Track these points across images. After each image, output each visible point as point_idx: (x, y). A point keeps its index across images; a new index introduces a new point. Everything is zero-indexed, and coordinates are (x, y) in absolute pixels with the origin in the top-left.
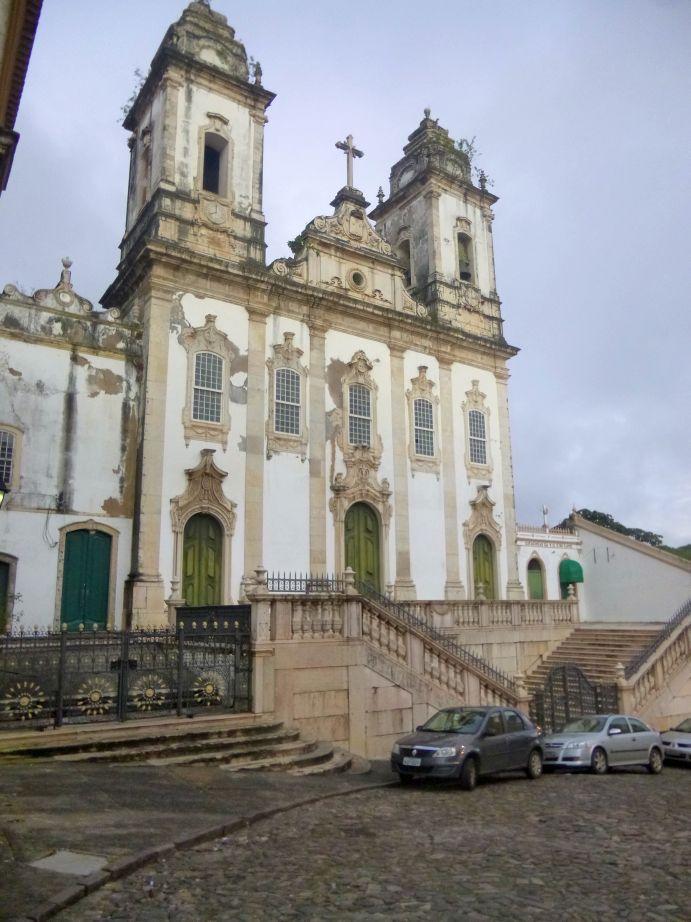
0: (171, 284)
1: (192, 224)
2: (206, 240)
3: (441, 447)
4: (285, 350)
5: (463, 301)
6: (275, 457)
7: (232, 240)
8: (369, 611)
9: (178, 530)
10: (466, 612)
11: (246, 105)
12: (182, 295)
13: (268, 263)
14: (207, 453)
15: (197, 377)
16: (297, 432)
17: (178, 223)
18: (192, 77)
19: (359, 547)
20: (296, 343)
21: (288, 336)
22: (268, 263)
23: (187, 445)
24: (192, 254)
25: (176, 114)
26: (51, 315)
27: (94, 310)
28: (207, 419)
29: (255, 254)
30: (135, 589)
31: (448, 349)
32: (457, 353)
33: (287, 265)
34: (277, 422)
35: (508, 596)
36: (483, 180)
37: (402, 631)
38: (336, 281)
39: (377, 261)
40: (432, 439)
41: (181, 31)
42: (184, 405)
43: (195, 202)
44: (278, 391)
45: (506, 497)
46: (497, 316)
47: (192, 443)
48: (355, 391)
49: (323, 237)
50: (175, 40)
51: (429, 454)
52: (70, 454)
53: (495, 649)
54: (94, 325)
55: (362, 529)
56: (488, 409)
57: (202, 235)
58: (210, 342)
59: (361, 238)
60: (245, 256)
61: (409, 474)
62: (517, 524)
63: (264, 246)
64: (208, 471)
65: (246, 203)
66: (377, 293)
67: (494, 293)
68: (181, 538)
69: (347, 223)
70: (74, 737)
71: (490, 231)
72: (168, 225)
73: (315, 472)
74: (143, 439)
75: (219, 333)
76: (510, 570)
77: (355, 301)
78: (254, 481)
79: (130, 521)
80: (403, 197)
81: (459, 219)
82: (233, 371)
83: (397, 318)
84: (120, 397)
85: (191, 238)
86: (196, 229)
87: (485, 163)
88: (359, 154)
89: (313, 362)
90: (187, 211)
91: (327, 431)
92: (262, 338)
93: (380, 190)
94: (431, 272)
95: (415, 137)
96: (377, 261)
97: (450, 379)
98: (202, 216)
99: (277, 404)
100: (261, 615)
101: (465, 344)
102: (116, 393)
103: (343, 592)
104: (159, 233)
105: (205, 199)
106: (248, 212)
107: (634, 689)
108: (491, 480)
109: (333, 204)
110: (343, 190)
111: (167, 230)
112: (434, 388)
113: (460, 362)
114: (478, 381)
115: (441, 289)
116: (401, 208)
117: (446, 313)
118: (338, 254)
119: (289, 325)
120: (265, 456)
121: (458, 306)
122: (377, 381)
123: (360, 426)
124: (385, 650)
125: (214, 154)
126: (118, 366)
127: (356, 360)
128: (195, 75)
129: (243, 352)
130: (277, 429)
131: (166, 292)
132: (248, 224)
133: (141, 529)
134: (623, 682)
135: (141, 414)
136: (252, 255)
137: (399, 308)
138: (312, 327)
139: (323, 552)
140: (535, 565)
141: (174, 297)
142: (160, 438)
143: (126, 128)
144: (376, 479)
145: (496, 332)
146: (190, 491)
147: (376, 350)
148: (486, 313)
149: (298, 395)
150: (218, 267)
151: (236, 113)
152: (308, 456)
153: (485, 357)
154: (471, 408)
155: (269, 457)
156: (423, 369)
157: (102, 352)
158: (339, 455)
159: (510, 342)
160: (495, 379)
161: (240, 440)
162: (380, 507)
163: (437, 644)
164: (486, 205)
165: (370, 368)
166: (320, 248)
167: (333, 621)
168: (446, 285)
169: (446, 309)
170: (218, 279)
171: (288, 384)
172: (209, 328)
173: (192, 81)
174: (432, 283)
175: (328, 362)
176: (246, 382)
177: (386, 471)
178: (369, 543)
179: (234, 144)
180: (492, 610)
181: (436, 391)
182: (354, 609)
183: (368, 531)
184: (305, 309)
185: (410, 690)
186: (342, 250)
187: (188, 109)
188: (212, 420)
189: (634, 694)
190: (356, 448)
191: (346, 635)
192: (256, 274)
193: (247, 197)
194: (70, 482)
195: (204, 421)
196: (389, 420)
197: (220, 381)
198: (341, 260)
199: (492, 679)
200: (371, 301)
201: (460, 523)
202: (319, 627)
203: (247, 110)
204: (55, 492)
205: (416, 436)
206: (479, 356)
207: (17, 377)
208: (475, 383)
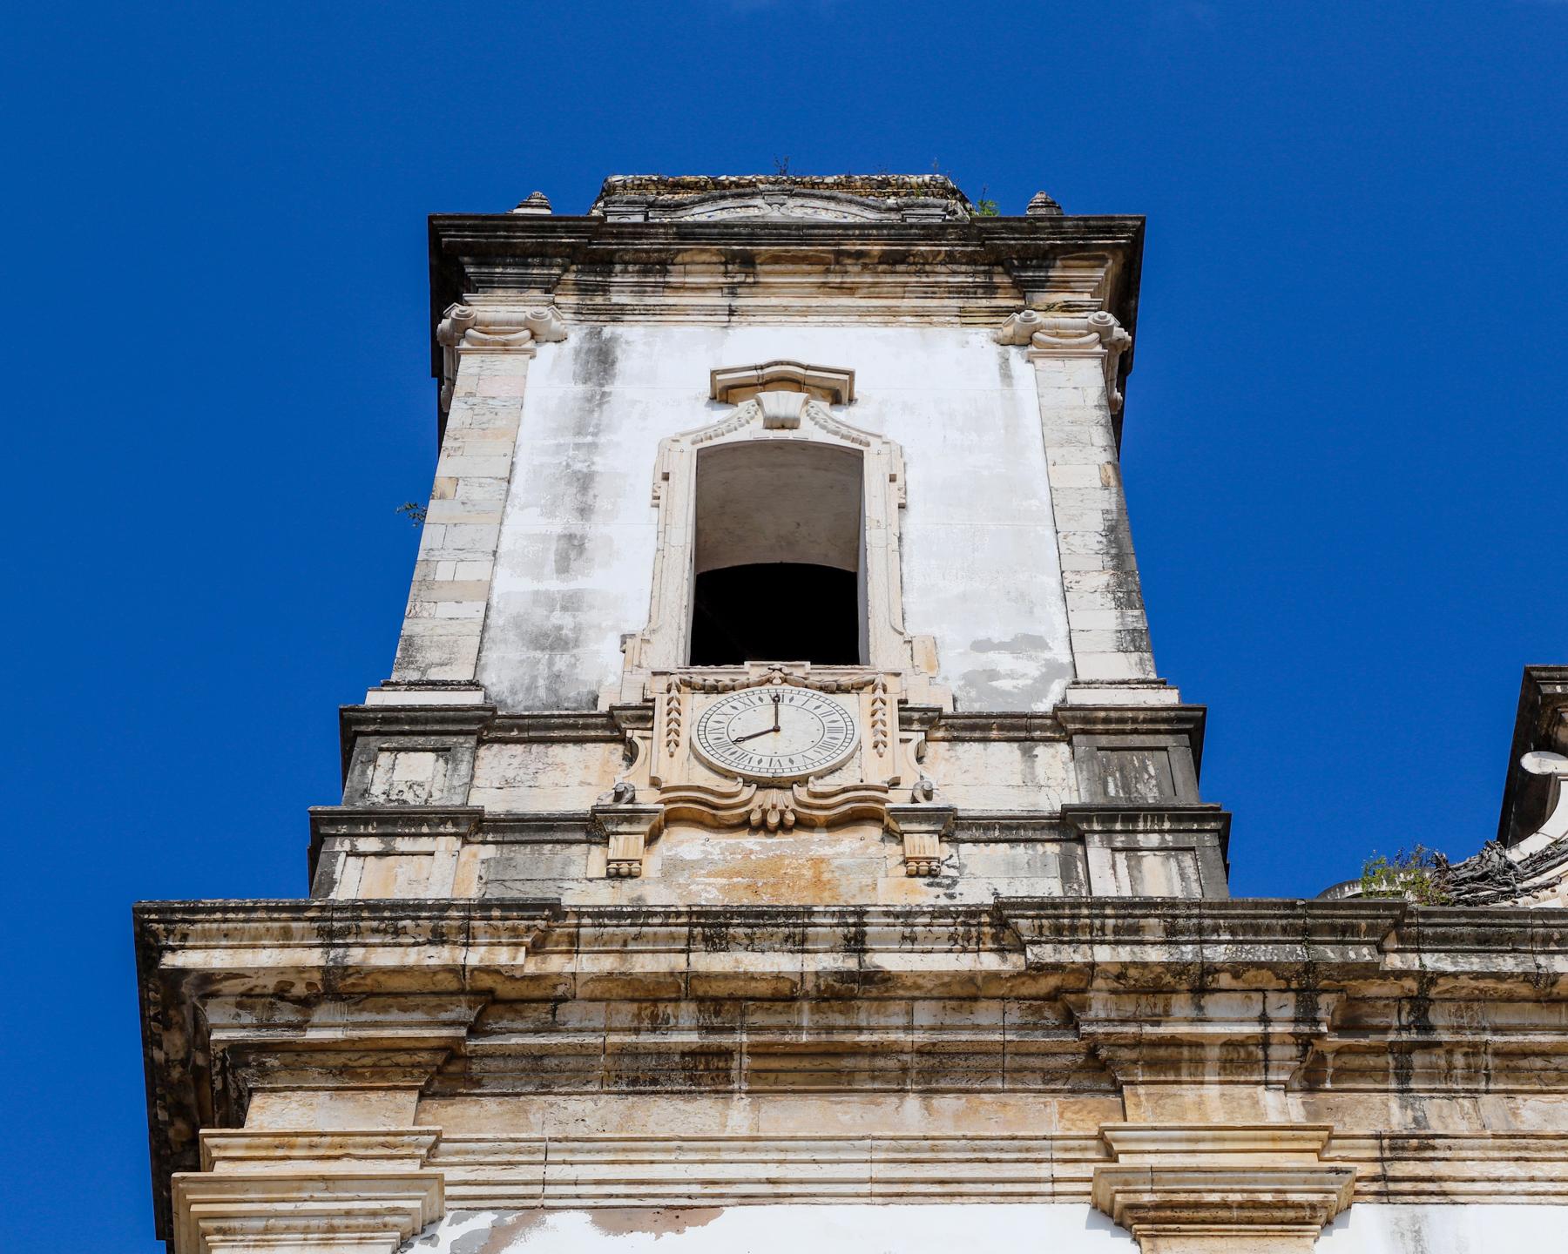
7: (924, 843)
170: (831, 1070)
173: (617, 314)
193: (1030, 643)
203: (981, 339)
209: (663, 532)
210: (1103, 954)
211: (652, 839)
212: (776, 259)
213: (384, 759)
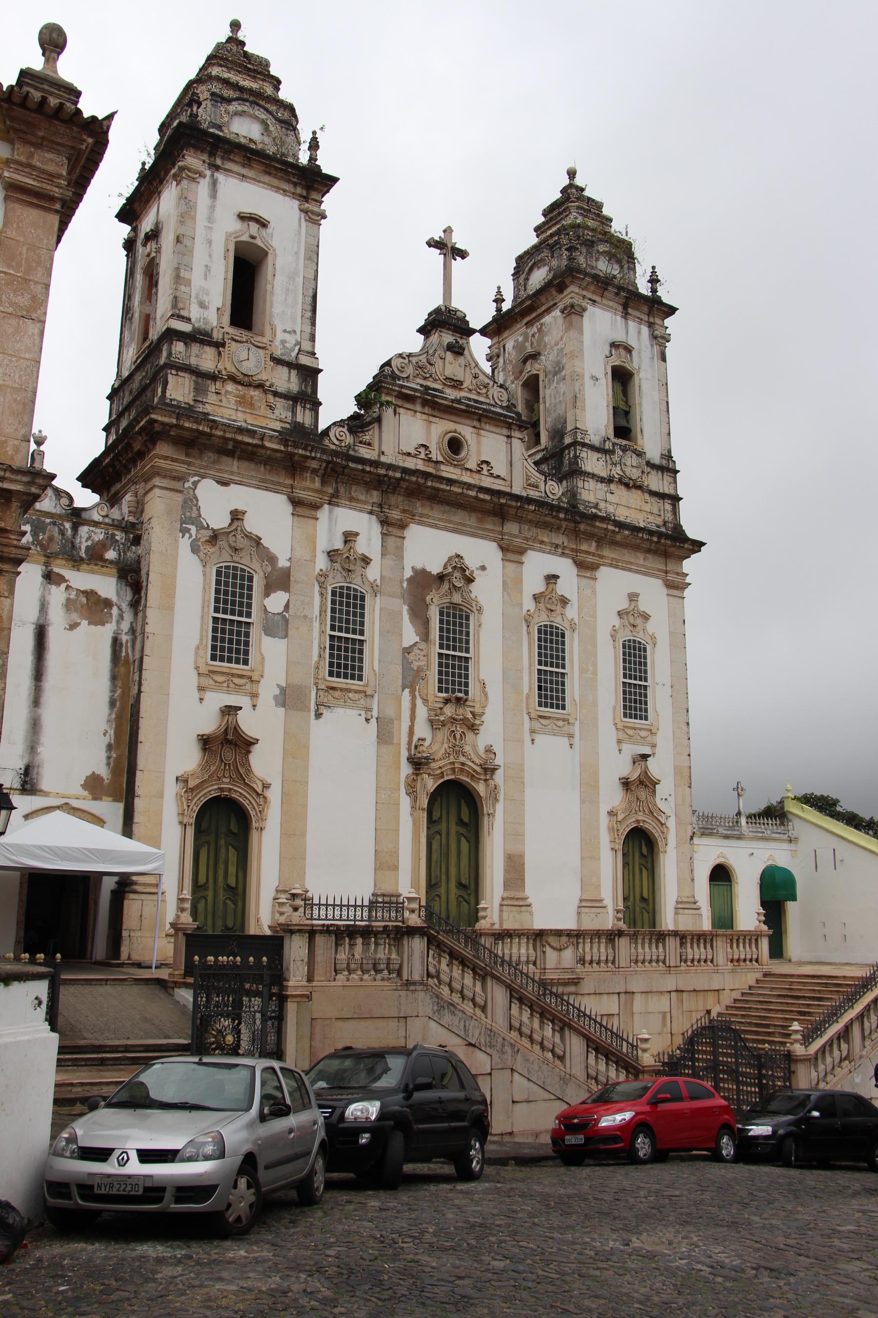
0: (182, 468)
2: (233, 400)
3: (577, 698)
4: (346, 557)
5: (616, 471)
7: (271, 398)
8: (438, 946)
9: (185, 820)
10: (595, 946)
11: (294, 196)
12: (199, 481)
13: (322, 426)
14: (230, 711)
15: (217, 600)
16: (360, 678)
17: (194, 378)
18: (219, 162)
20: (361, 547)
22: (322, 426)
23: (201, 699)
24: (214, 424)
25: (194, 218)
27: (78, 504)
28: (230, 660)
29: (303, 417)
30: (126, 902)
31: (592, 547)
32: (607, 552)
33: (350, 431)
34: (331, 664)
35: (676, 922)
36: (654, 280)
37: (482, 975)
38: (422, 450)
39: (486, 417)
40: (563, 684)
41: (203, 92)
42: (197, 642)
43: (219, 345)
44: (333, 619)
45: (677, 770)
46: (672, 492)
47: (209, 696)
48: (448, 615)
49: (402, 386)
50: (195, 109)
52: (39, 711)
53: (638, 1000)
54: (75, 528)
56: (653, 638)
57: (227, 392)
58: (236, 550)
59: (461, 383)
60: (289, 420)
61: (527, 738)
62: (694, 812)
63: (316, 404)
64: (230, 737)
65: (291, 340)
66: (484, 466)
67: (668, 456)
68: (190, 831)
69: (440, 362)
70: (70, 1088)
71: (664, 359)
72: (180, 380)
73: (385, 736)
74: (140, 692)
75: (248, 536)
76: (681, 885)
77: (450, 482)
78: (296, 751)
79: (120, 807)
80: (531, 309)
81: (614, 345)
82: (268, 590)
83: (514, 504)
84: (107, 632)
85: (212, 398)
86: (219, 384)
87: (657, 256)
88: (463, 254)
89: (385, 574)
90: (206, 360)
91: (404, 677)
92: (312, 541)
93: (499, 292)
94: (569, 428)
95: (553, 211)
96: (486, 417)
97: (594, 592)
98: (226, 366)
99: (332, 637)
100: (296, 950)
101: (618, 538)
102: (103, 625)
103: (403, 922)
104: (168, 395)
105: (233, 339)
106: (294, 354)
107: (816, 1059)
108: (654, 746)
109: (421, 330)
110: (437, 311)
111: (179, 389)
112: (568, 606)
113: (611, 565)
114: (637, 595)
115: (583, 455)
116: (529, 324)
117: (591, 493)
118: (426, 410)
119: (350, 520)
120: (313, 713)
121: (609, 480)
122: (482, 601)
123: (453, 667)
124: (456, 998)
125: (247, 269)
126: (106, 585)
127: (450, 570)
128: (223, 158)
129: (283, 563)
130: (331, 674)
132: (294, 373)
133: (136, 820)
134: (798, 1049)
135: (137, 656)
136: (299, 419)
137: (517, 490)
138: (385, 522)
139: (395, 853)
140: (721, 875)
141: (187, 485)
142: (164, 690)
143: (120, 221)
144: (474, 747)
145: (669, 517)
146: (205, 766)
148: (654, 487)
149: (362, 624)
150: (250, 440)
151: (278, 207)
152: (375, 713)
153: (650, 556)
154: (625, 635)
155: (318, 715)
156: (551, 579)
157: (84, 566)
158: (422, 712)
159: (691, 534)
160: (665, 591)
161: (277, 691)
162: (481, 788)
163: (531, 991)
164: (658, 321)
165: (470, 580)
166: (400, 403)
167: (389, 959)
168: (592, 448)
169: (591, 484)
171: (347, 608)
172: (236, 530)
173: (217, 168)
174: (569, 446)
175: (408, 573)
176: (287, 607)
177: (492, 733)
178: (463, 840)
179: (275, 255)
180: (636, 943)
181: (571, 612)
182: (418, 944)
183: (460, 822)
184: (375, 496)
185: (488, 1050)
186: (432, 404)
187: (212, 208)
188: (237, 662)
189: (816, 1066)
190: (447, 701)
191: (405, 977)
192: (305, 449)
194: (39, 750)
195: (226, 664)
196: (499, 658)
197: (249, 606)
198: (432, 419)
199: (605, 1038)
201: (604, 809)
202: (371, 966)
203: (296, 204)
204: (20, 764)
205: (539, 680)
206: (641, 556)
208: (633, 597)
209: (227, 266)
210: (300, 451)
212: (255, 160)
213: (174, 342)
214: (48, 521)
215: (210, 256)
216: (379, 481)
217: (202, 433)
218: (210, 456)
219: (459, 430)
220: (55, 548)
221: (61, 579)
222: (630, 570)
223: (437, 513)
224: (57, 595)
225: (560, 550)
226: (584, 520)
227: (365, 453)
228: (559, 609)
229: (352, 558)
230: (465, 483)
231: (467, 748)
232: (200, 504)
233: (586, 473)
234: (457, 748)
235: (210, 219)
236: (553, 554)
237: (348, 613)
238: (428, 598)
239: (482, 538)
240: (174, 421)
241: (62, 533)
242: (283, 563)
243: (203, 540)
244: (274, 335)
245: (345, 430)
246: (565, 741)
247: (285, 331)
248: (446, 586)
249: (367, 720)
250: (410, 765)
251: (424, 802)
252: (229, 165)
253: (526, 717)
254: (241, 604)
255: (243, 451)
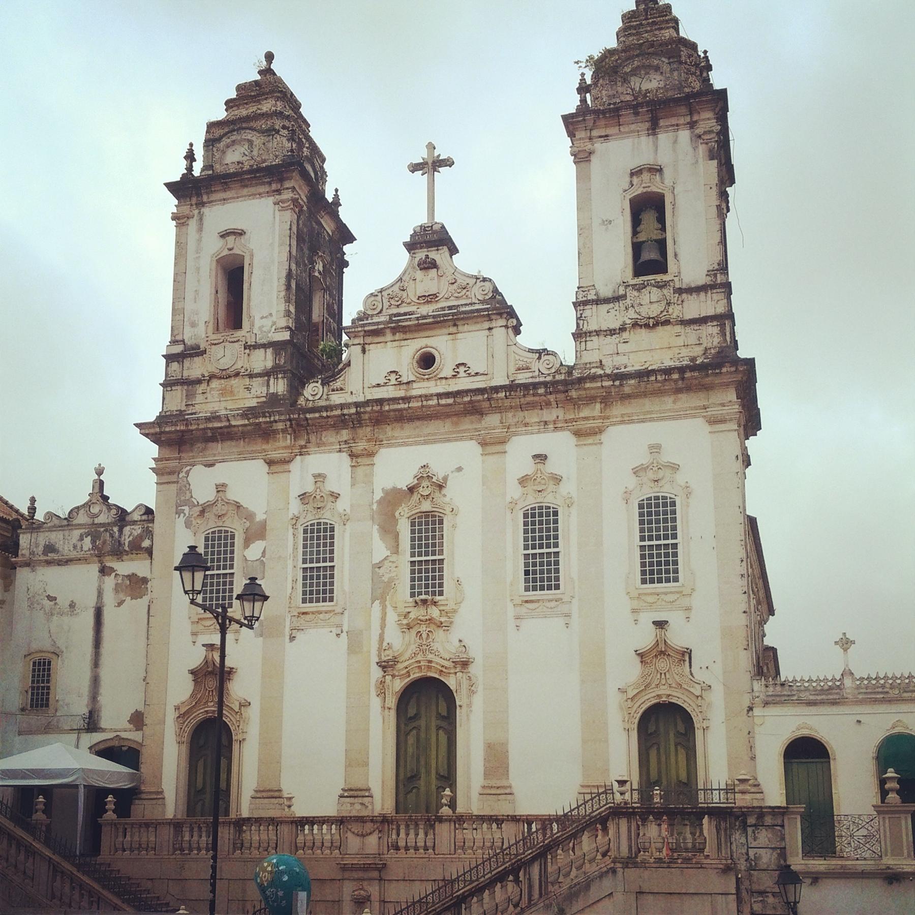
0: (173, 464)
1: (199, 382)
2: (215, 393)
6: (299, 636)
17: (186, 387)
19: (428, 740)
21: (319, 478)
26: (82, 531)
31: (596, 409)
32: (618, 410)
34: (304, 593)
38: (393, 377)
44: (304, 553)
48: (420, 524)
49: (364, 325)
51: (549, 588)
55: (434, 714)
65: (267, 323)
66: (462, 369)
68: (185, 748)
72: (174, 393)
73: (355, 646)
78: (273, 673)
82: (247, 543)
83: (480, 397)
85: (199, 398)
86: (203, 386)
99: (305, 569)
101: (627, 390)
113: (622, 422)
119: (327, 463)
127: (416, 482)
128: (208, 193)
129: (260, 517)
130: (304, 601)
131: (170, 473)
136: (271, 391)
138: (352, 456)
141: (180, 476)
146: (193, 696)
147: (453, 457)
150: (219, 425)
155: (292, 638)
156: (541, 458)
157: (125, 557)
158: (392, 617)
162: (451, 682)
168: (598, 301)
175: (378, 495)
181: (568, 488)
184: (345, 434)
186: (400, 328)
187: (199, 240)
196: (480, 551)
197: (232, 559)
198: (403, 343)
200: (454, 386)
203: (271, 200)
207: (52, 603)
210: (261, 420)
211: (208, 385)
214: (102, 529)
215: (198, 281)
216: (342, 421)
217: (182, 431)
218: (200, 445)
219: (429, 344)
220: (108, 548)
221: (112, 570)
222: (652, 420)
223: (408, 430)
224: (109, 582)
225: (551, 426)
226: (570, 387)
227: (337, 399)
228: (551, 487)
229: (318, 497)
230: (420, 396)
231: (435, 646)
232: (191, 487)
233: (586, 333)
234: (425, 647)
235: (198, 250)
236: (544, 432)
237: (318, 545)
238: (397, 514)
239: (456, 440)
240: (158, 430)
241: (112, 536)
242: (260, 517)
243: (195, 515)
244: (252, 325)
245: (319, 385)
246: (561, 621)
247: (262, 318)
248: (416, 497)
249: (338, 635)
250: (380, 669)
251: (392, 702)
252: (214, 197)
253: (510, 606)
254: (225, 560)
255: (221, 434)
